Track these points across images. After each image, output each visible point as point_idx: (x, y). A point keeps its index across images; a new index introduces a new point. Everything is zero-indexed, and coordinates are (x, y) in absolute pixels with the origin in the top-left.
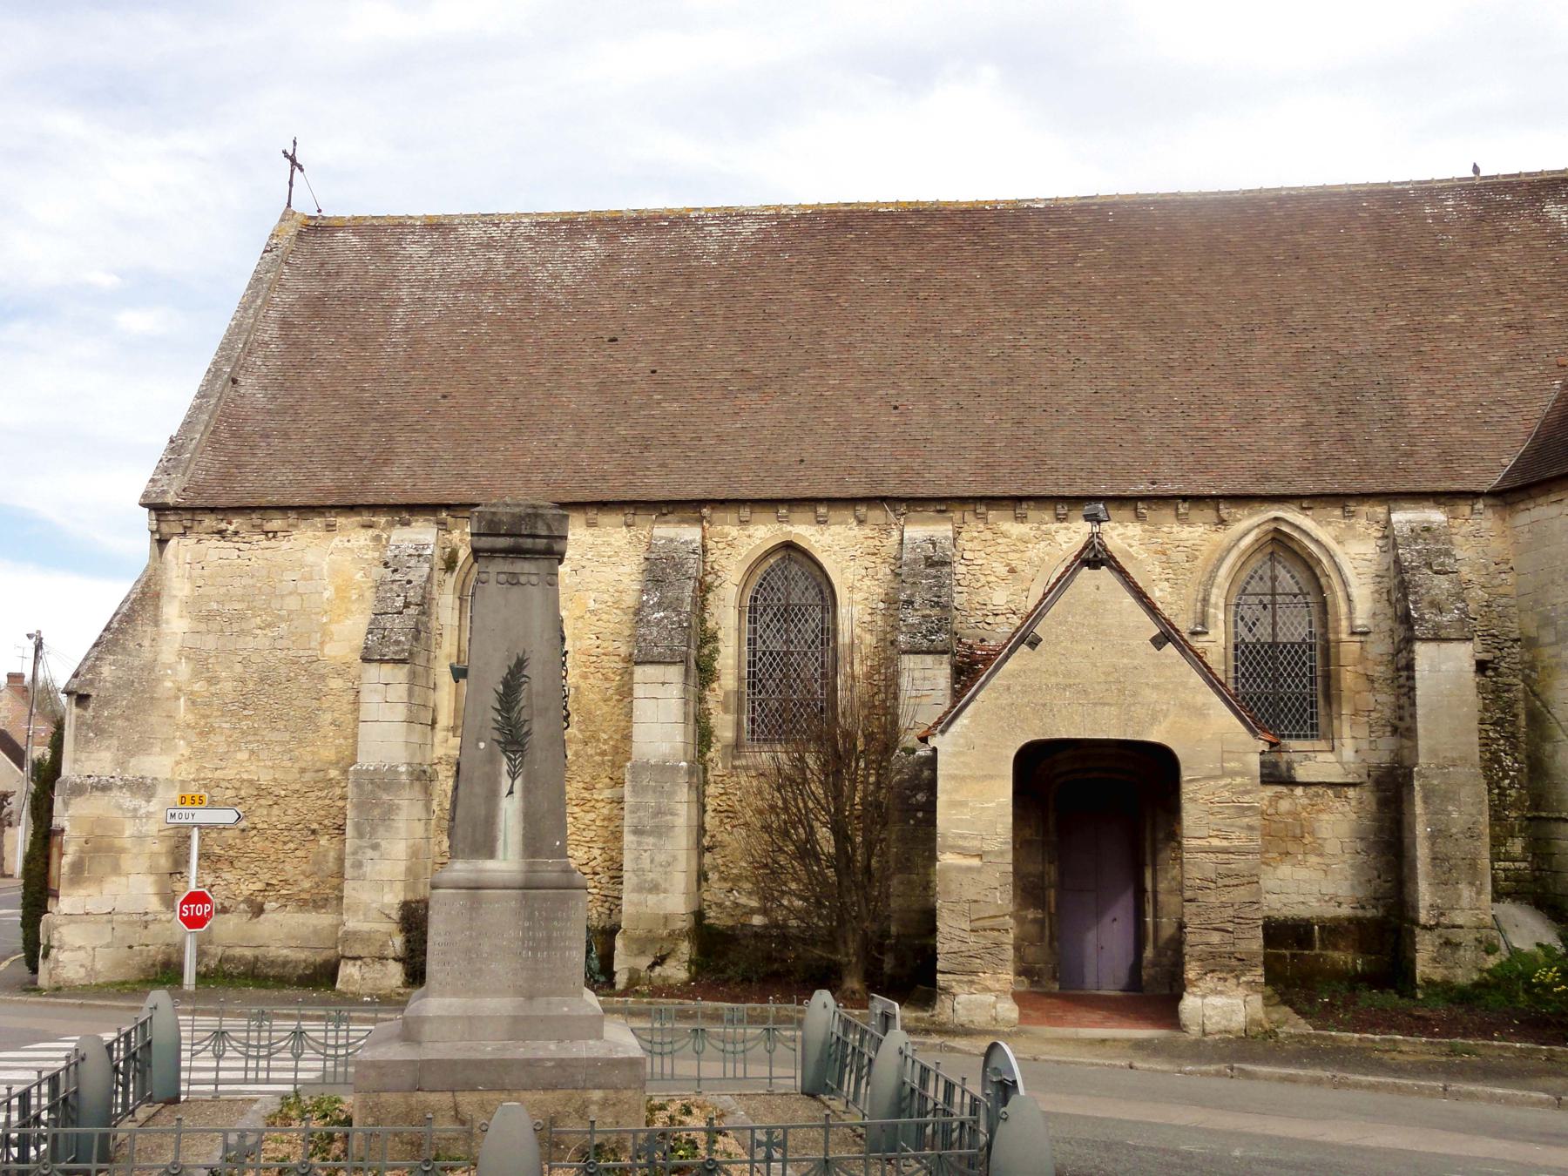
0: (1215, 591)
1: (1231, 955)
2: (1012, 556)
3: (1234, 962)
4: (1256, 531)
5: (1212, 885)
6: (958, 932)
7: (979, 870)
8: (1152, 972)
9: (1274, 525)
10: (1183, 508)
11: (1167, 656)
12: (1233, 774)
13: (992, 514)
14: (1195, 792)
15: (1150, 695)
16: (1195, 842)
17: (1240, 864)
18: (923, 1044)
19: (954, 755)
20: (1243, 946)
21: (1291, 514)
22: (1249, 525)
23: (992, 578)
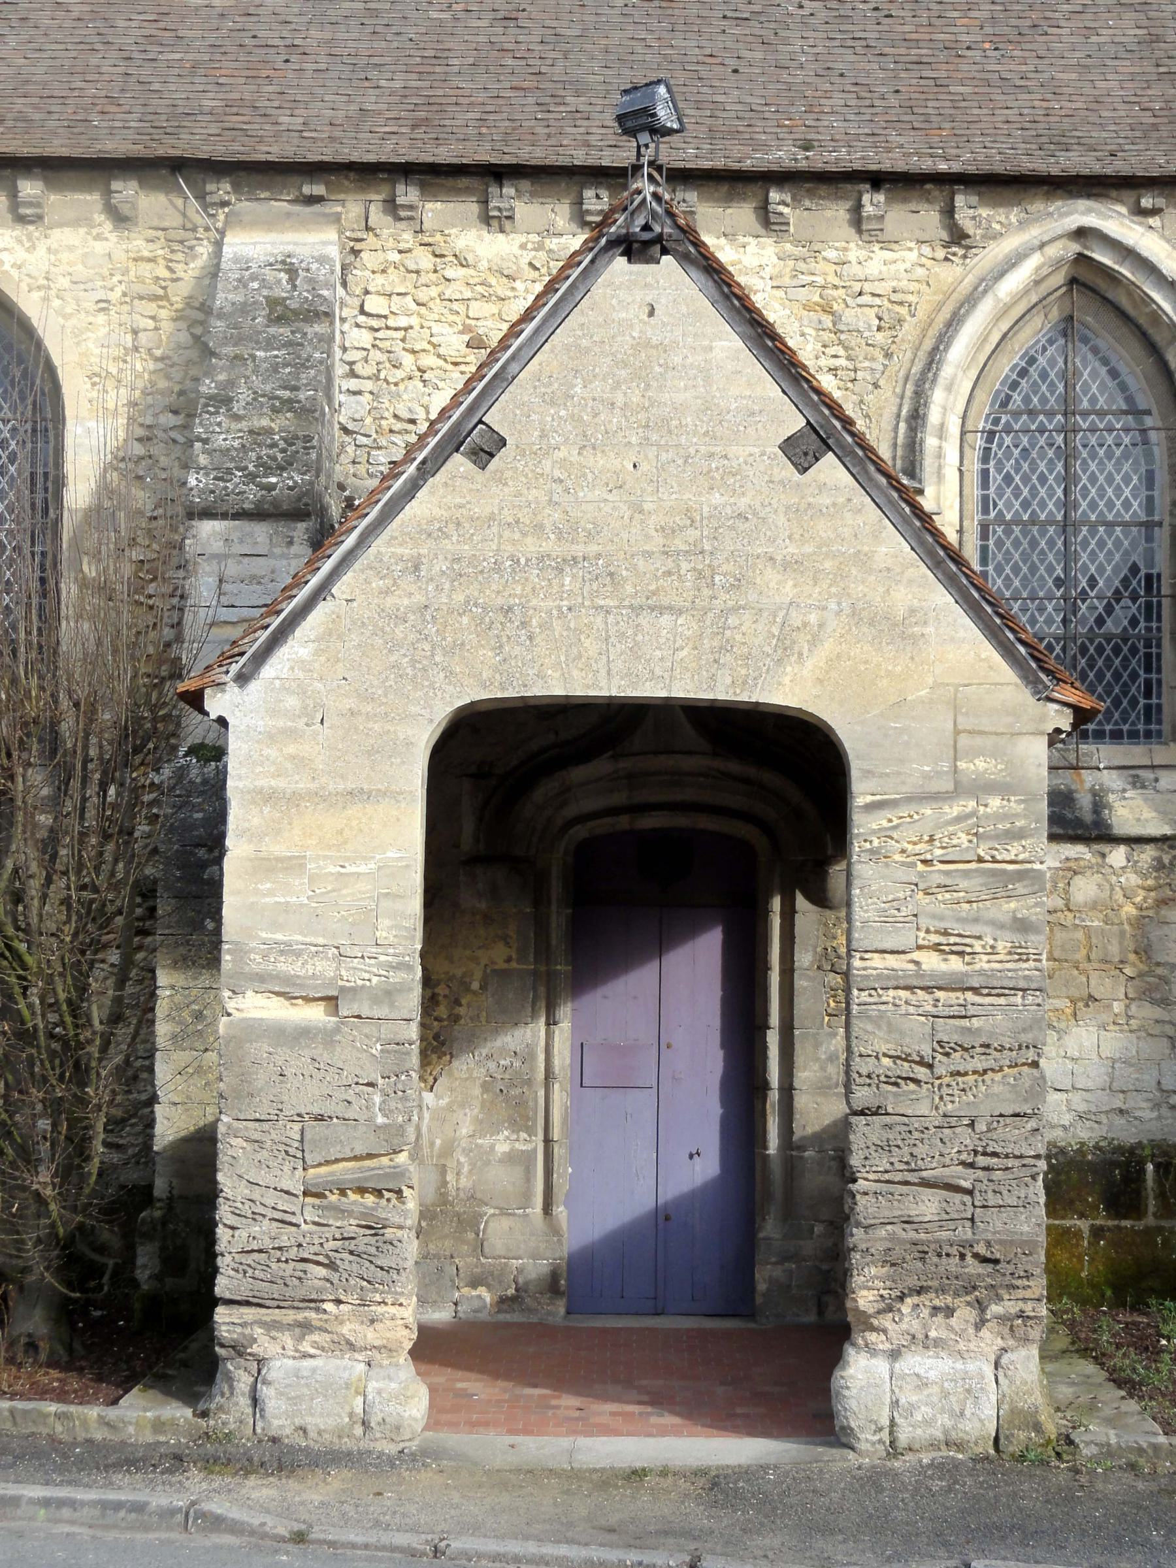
0: (938, 396)
1: (964, 1250)
2: (476, 308)
3: (973, 1267)
4: (1035, 260)
5: (921, 1072)
6: (271, 1198)
7: (329, 1038)
8: (778, 1272)
9: (1075, 247)
10: (873, 202)
11: (822, 487)
12: (982, 788)
13: (433, 211)
14: (886, 834)
15: (778, 588)
16: (877, 962)
17: (995, 1019)
18: (139, 1508)
19: (271, 737)
20: (995, 1224)
21: (1113, 220)
22: (1025, 247)
23: (429, 360)
